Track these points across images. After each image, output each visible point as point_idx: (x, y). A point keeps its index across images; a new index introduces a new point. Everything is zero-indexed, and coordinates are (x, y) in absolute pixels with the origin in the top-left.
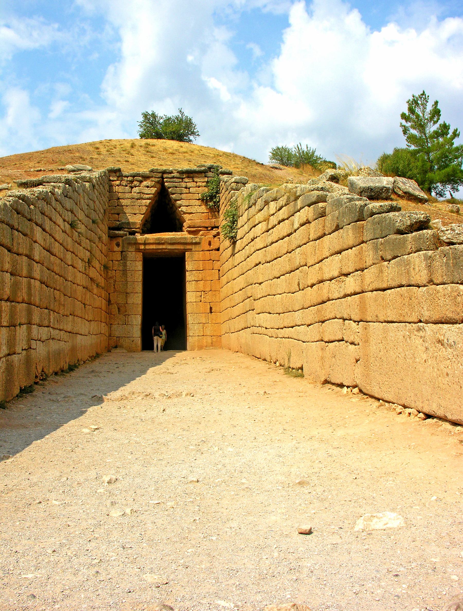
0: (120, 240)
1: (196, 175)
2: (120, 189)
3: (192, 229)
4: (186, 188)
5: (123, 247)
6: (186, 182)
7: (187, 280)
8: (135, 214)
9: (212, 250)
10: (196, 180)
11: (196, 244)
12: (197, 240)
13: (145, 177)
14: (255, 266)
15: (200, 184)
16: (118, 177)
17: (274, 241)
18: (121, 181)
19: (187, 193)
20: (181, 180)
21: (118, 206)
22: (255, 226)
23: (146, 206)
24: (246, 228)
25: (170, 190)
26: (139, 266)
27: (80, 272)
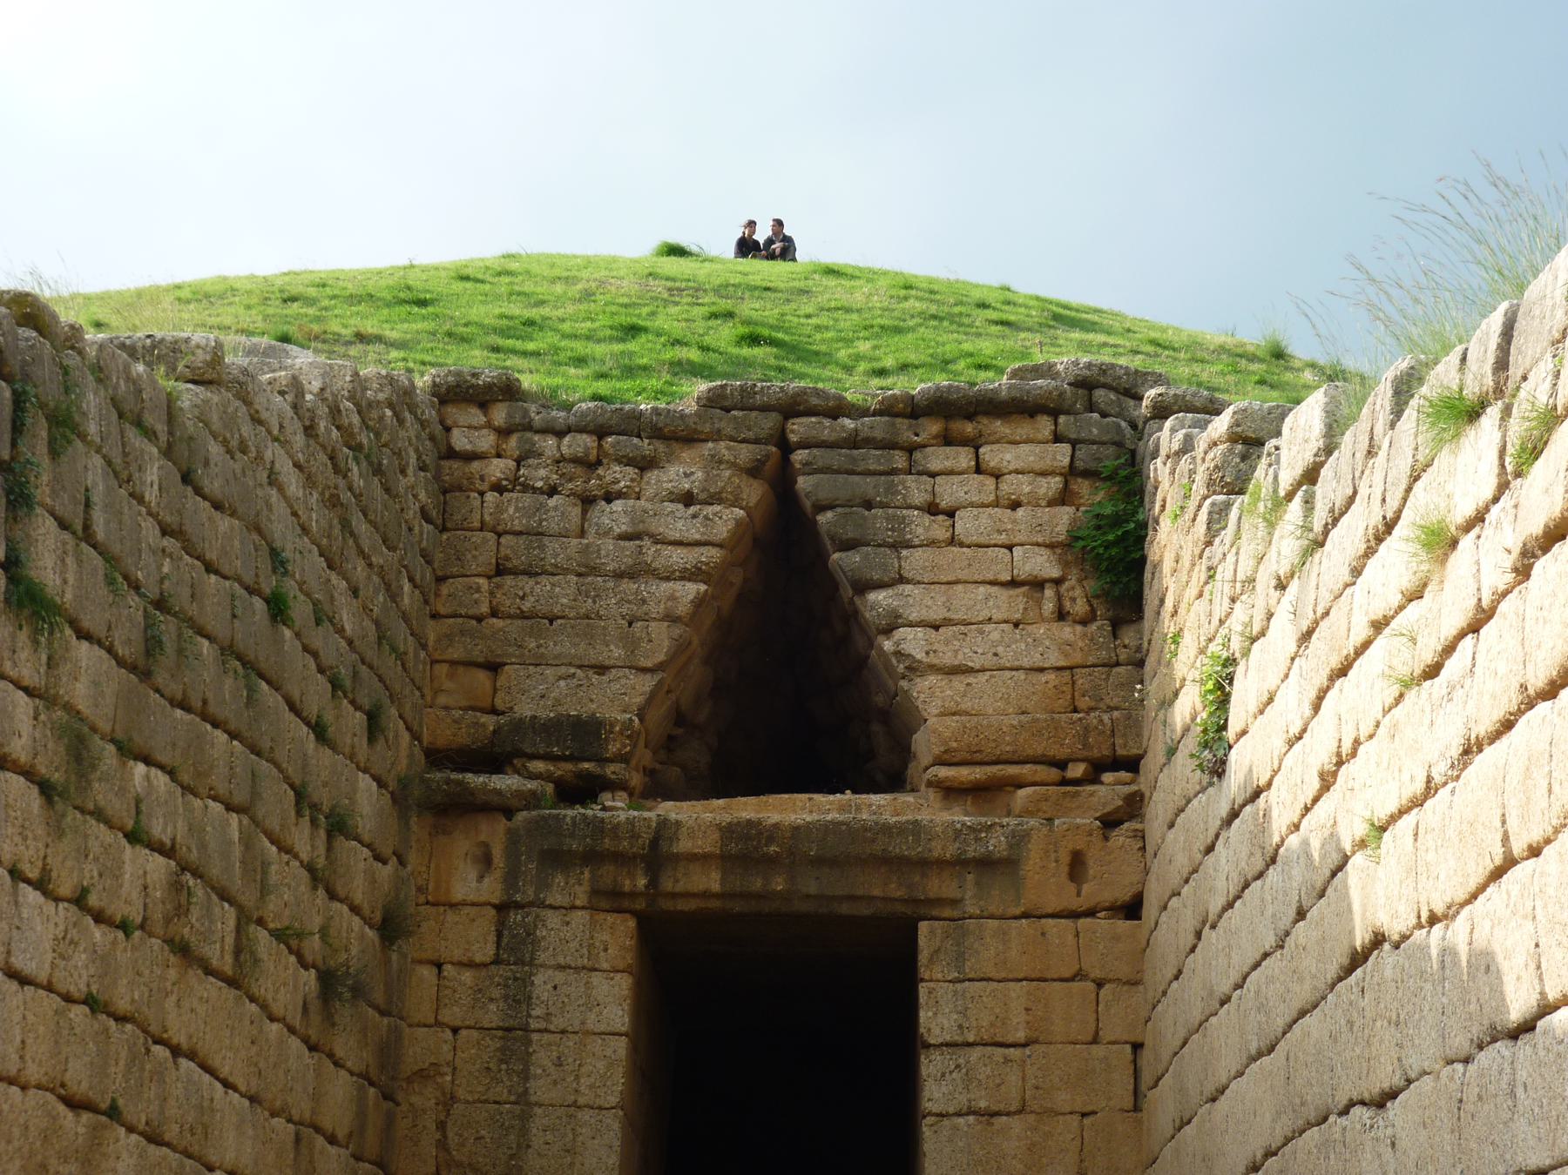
0: (494, 832)
1: (999, 427)
2: (514, 510)
4: (932, 509)
5: (511, 878)
6: (933, 475)
7: (927, 1105)
8: (602, 669)
9: (1091, 913)
10: (993, 455)
11: (986, 864)
12: (997, 844)
14: (1349, 970)
17: (1483, 728)
18: (519, 462)
19: (932, 543)
20: (899, 460)
21: (494, 613)
22: (1343, 672)
23: (671, 618)
24: (1292, 706)
25: (825, 518)
27: (24, 980)
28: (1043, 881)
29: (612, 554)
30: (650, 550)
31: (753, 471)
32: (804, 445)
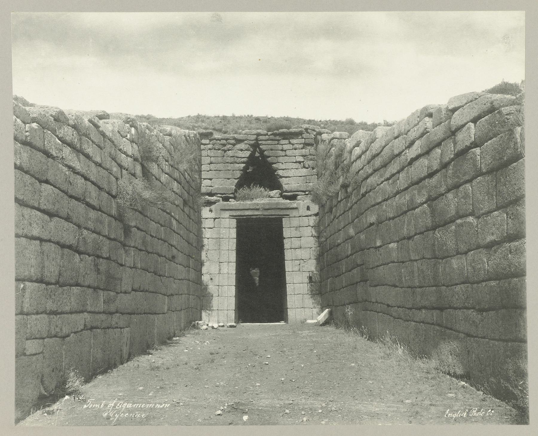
0: (213, 207)
3: (289, 194)
4: (282, 150)
6: (282, 145)
7: (285, 248)
8: (229, 179)
9: (310, 216)
12: (295, 205)
13: (239, 141)
15: (297, 146)
16: (211, 140)
19: (283, 156)
20: (276, 142)
26: (233, 233)
28: (303, 211)
29: (229, 160)
30: (236, 159)
31: (252, 145)
32: (261, 140)
